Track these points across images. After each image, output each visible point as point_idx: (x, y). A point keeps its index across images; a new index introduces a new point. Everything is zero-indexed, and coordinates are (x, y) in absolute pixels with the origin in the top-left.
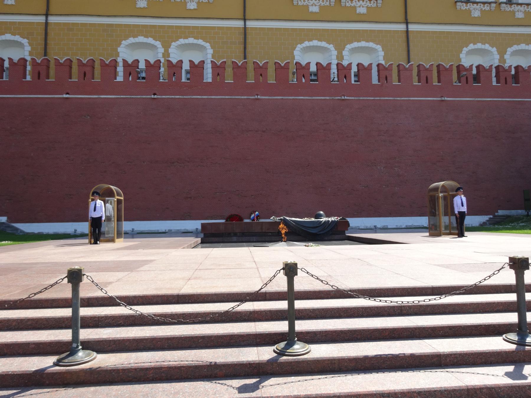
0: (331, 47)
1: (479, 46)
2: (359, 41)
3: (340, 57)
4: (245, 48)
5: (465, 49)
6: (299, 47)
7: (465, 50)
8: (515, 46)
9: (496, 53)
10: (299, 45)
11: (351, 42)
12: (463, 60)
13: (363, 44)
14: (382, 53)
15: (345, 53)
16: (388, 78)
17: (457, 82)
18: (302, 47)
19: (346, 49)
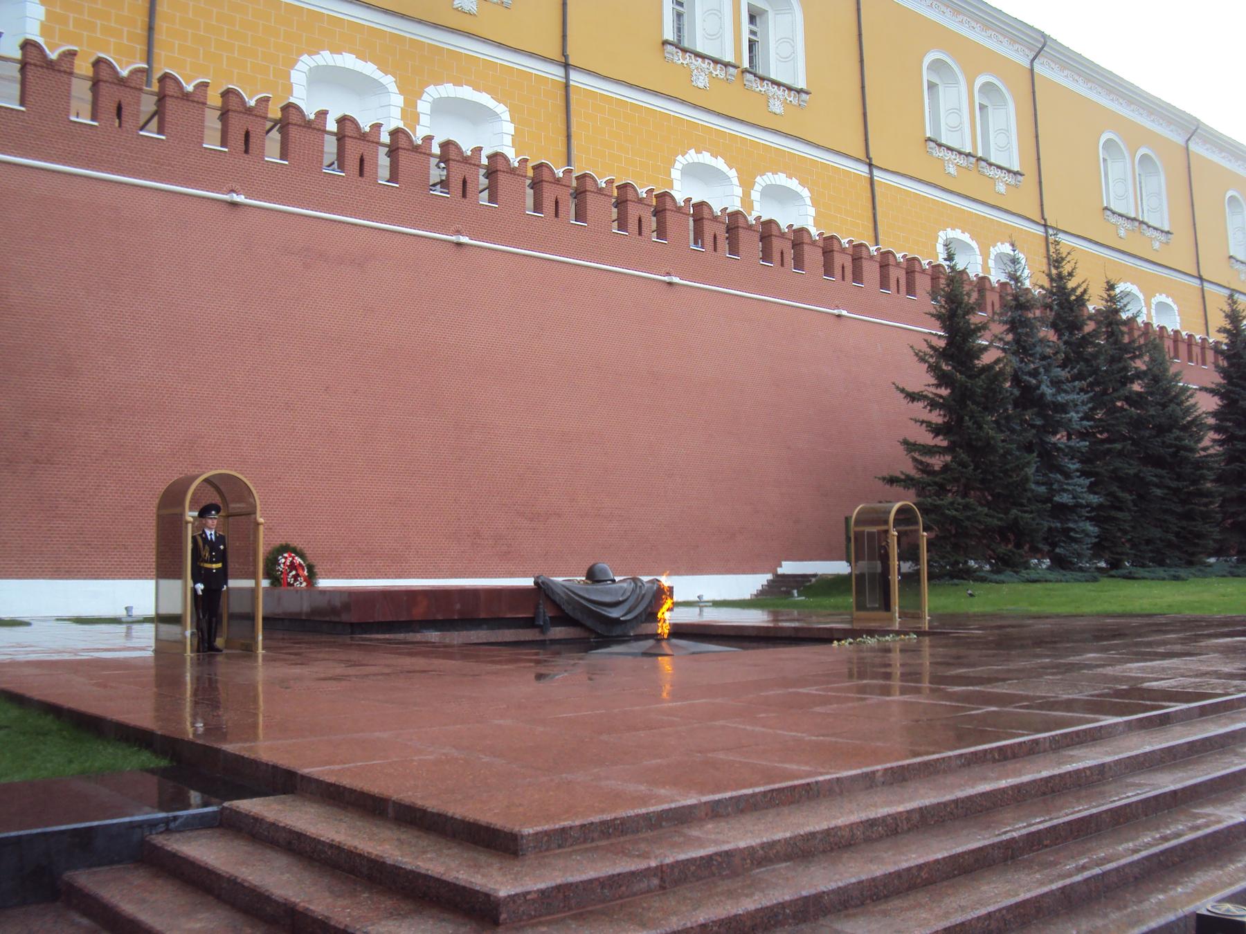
0: (388, 81)
1: (706, 158)
2: (458, 83)
3: (410, 113)
4: (151, 29)
5: (679, 158)
6: (306, 62)
7: (681, 161)
8: (770, 174)
9: (735, 181)
10: (305, 58)
11: (438, 82)
12: (677, 185)
13: (466, 92)
14: (509, 128)
15: (423, 106)
16: (125, 112)
17: (335, 166)
18: (313, 64)
19: (425, 96)
